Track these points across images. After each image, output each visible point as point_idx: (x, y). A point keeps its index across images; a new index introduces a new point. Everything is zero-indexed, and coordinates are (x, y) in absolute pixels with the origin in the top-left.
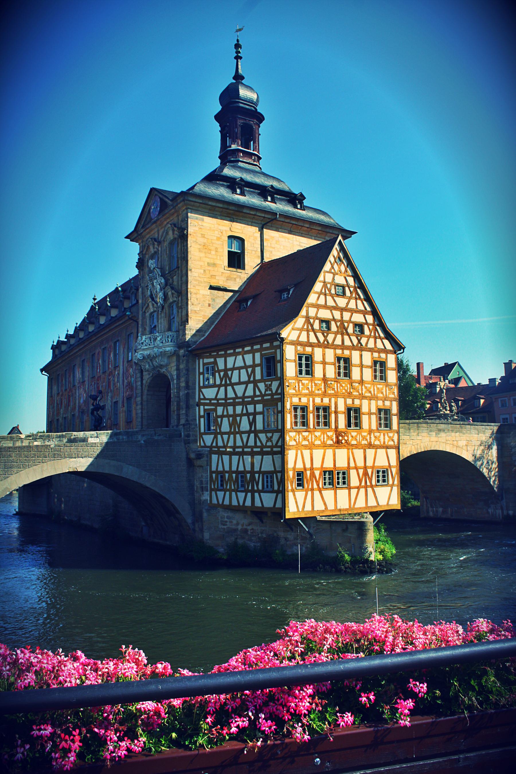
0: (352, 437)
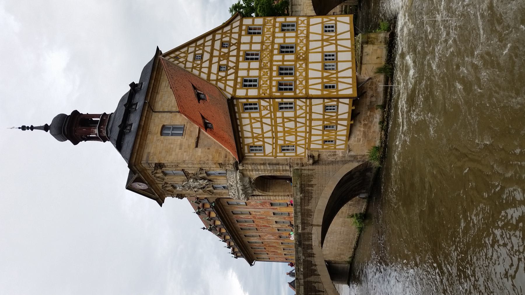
0: (300, 50)
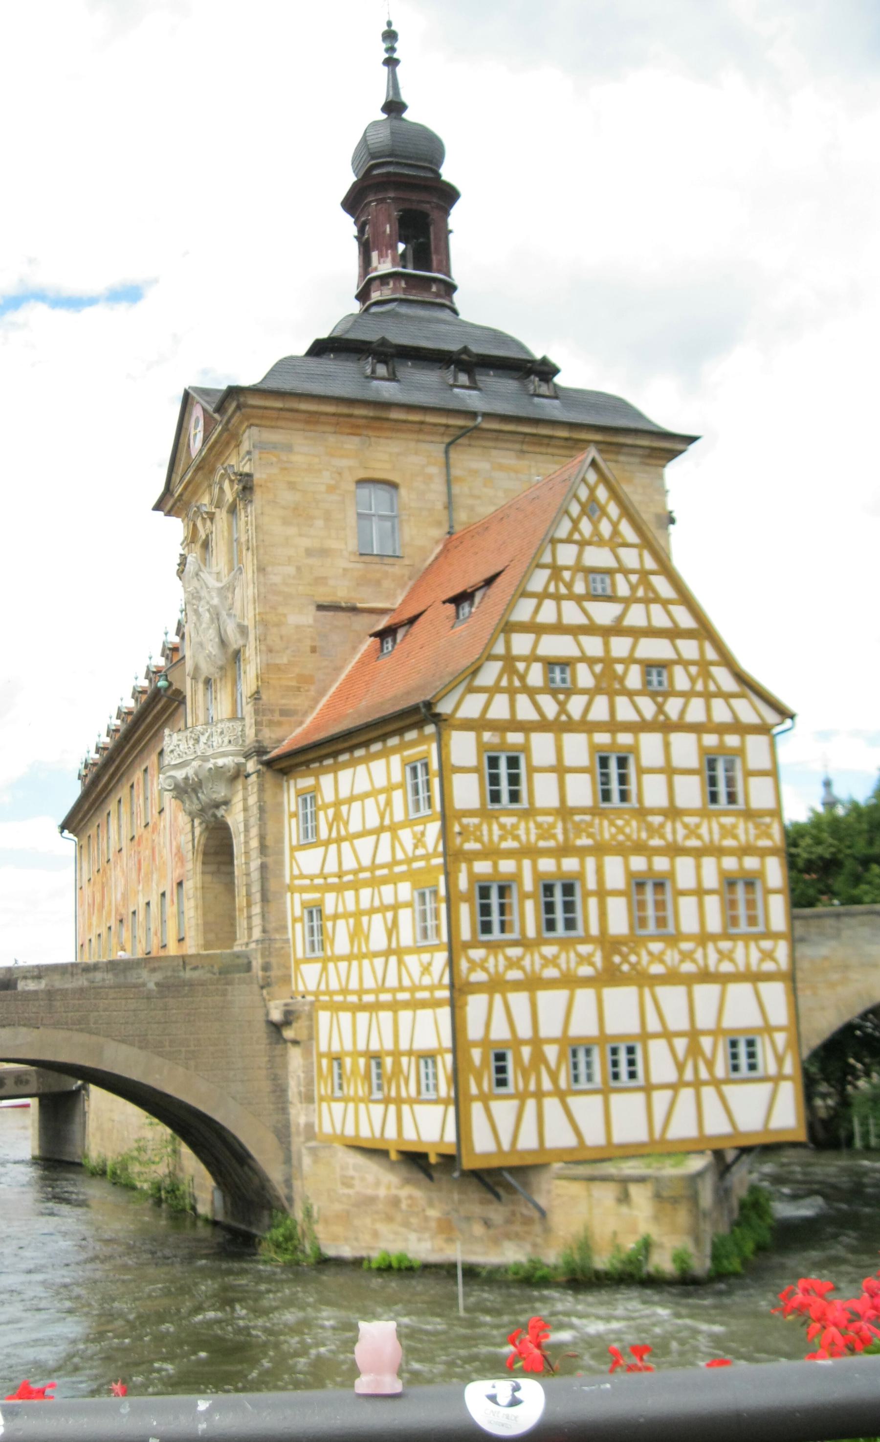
0: (650, 953)
